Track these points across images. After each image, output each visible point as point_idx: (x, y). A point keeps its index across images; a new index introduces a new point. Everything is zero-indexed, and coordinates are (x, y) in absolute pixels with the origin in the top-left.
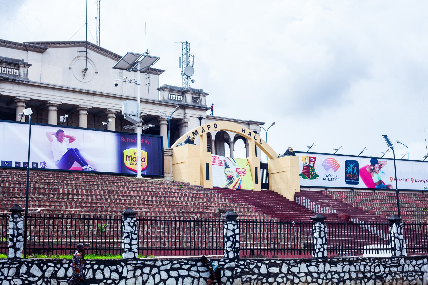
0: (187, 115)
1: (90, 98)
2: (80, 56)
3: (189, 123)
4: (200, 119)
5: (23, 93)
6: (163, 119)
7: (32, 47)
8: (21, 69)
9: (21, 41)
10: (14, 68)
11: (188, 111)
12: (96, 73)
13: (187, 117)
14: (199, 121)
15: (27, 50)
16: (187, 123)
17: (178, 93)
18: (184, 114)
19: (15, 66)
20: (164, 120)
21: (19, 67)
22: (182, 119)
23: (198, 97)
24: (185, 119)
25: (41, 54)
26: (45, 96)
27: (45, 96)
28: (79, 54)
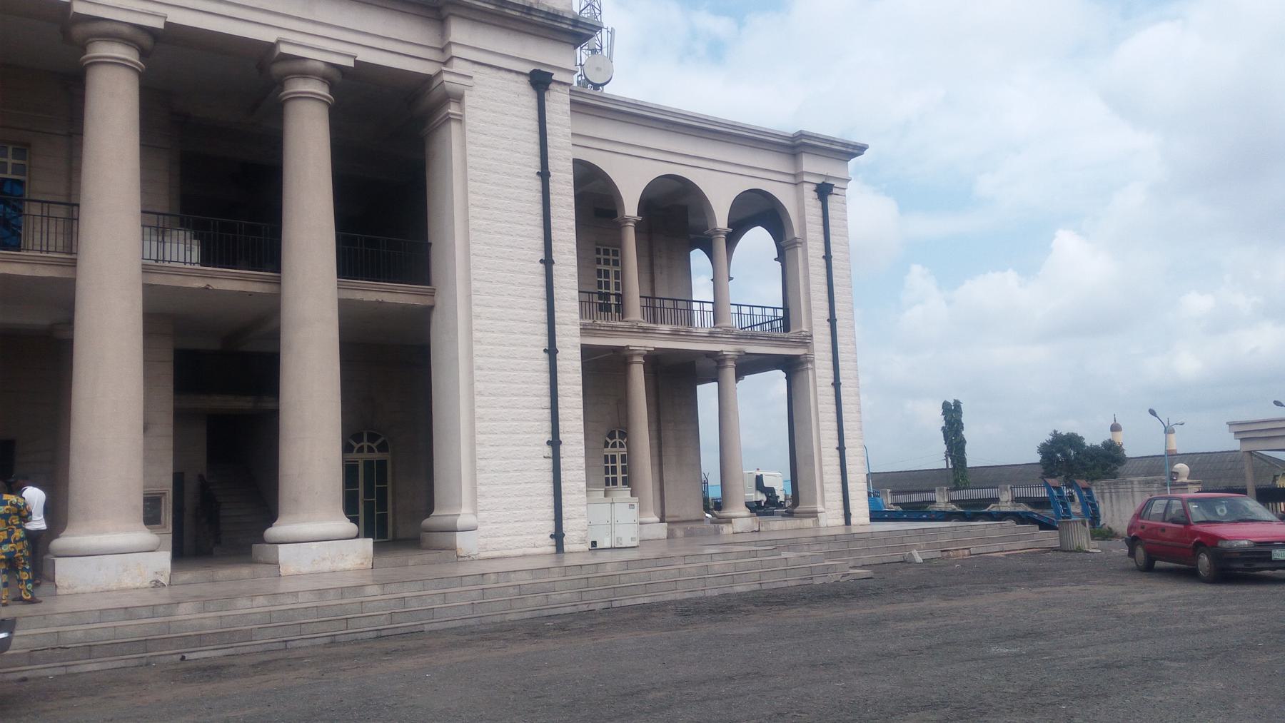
0: (455, 51)
3: (468, 100)
4: (540, 81)
13: (458, 66)
14: (529, 99)
16: (459, 98)
18: (443, 50)
20: (305, 74)
22: (426, 80)
24: (446, 77)
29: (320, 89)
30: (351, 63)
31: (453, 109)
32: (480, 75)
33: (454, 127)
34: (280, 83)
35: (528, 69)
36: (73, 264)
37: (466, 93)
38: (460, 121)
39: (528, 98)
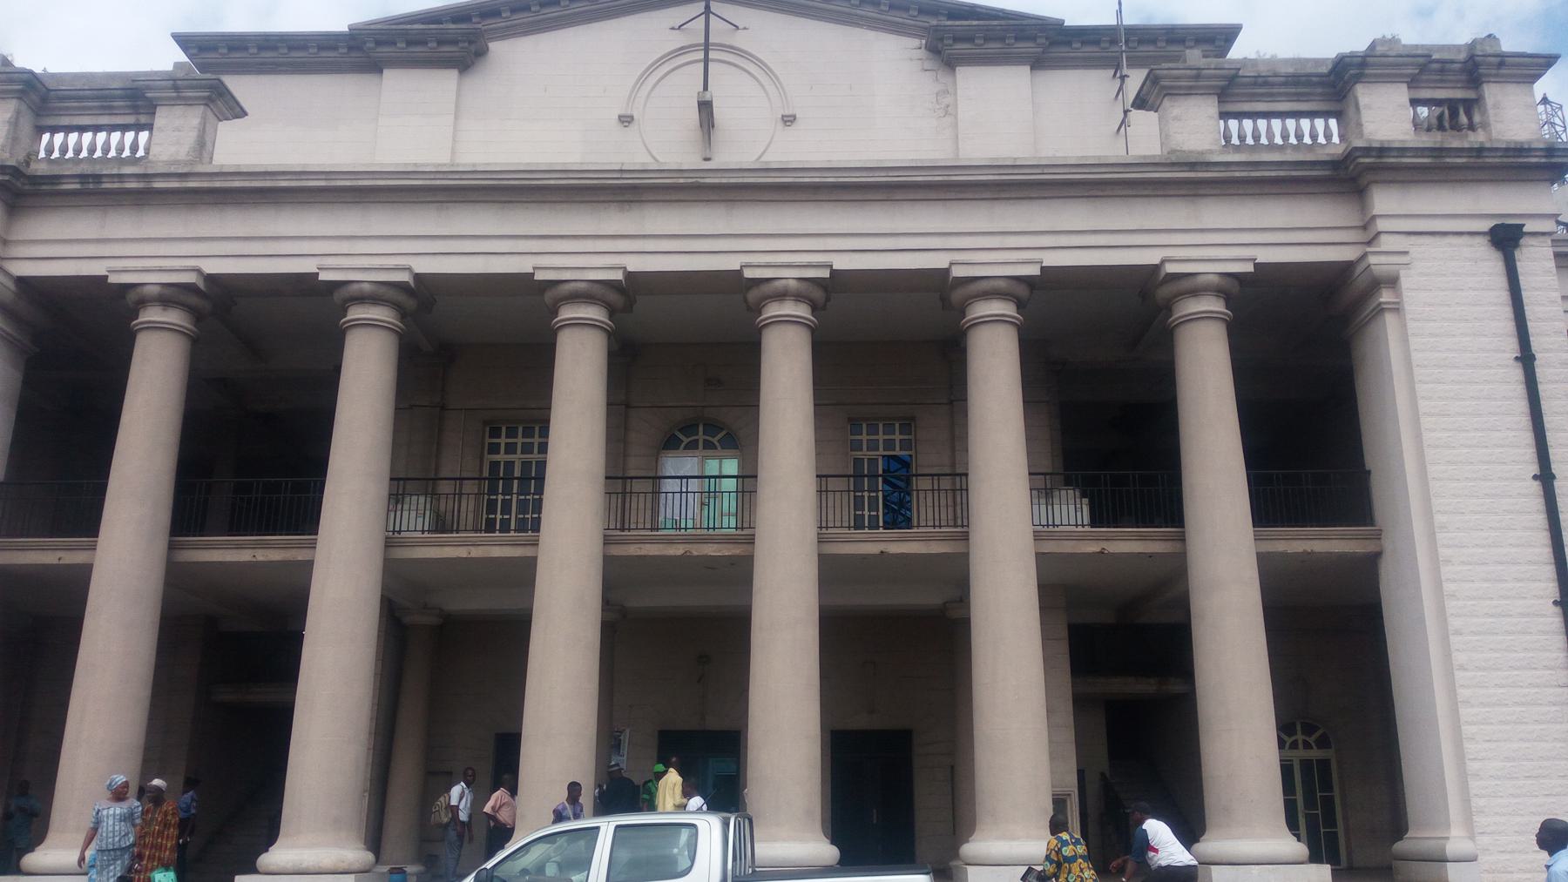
0: (1382, 225)
1: (614, 221)
2: (682, 51)
3: (1405, 282)
4: (1506, 238)
5: (163, 249)
6: (1187, 285)
7: (394, 43)
8: (162, 118)
9: (336, 21)
10: (130, 120)
11: (1385, 201)
12: (789, 120)
13: (1387, 243)
15: (374, 67)
16: (1393, 282)
17: (1298, 97)
18: (1365, 228)
19: (136, 110)
20: (1195, 292)
21: (151, 109)
22: (1346, 268)
23: (1470, 94)
24: (1372, 260)
25: (453, 74)
26: (306, 247)
27: (306, 247)
28: (679, 40)
29: (1215, 305)
30: (1249, 268)
31: (1386, 297)
32: (1418, 247)
33: (1389, 318)
34: (1167, 307)
35: (1485, 226)
36: (965, 537)
37: (1402, 273)
38: (1397, 309)
39: (1492, 263)
